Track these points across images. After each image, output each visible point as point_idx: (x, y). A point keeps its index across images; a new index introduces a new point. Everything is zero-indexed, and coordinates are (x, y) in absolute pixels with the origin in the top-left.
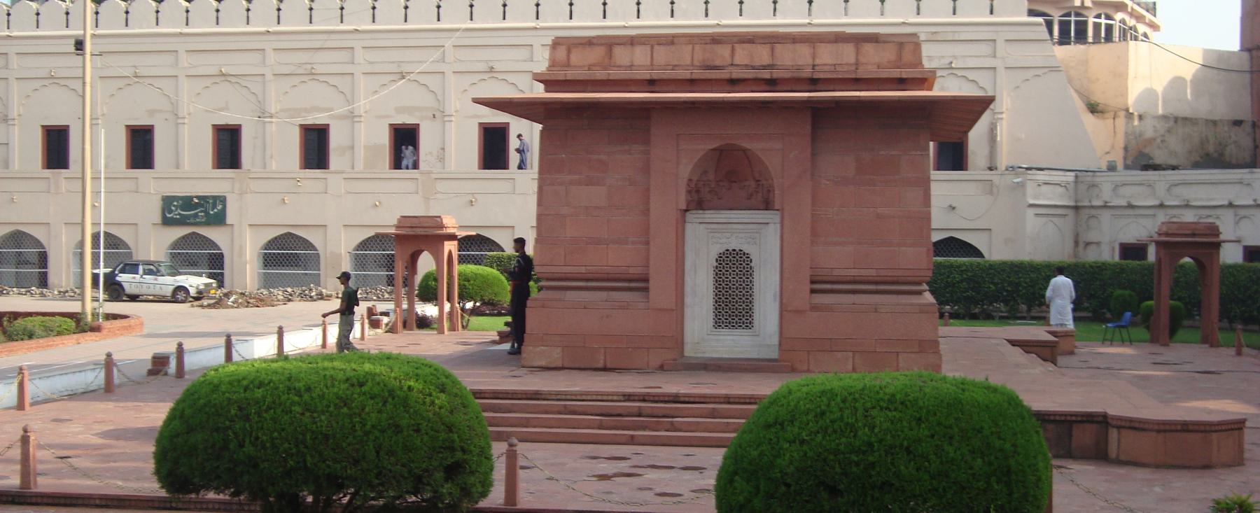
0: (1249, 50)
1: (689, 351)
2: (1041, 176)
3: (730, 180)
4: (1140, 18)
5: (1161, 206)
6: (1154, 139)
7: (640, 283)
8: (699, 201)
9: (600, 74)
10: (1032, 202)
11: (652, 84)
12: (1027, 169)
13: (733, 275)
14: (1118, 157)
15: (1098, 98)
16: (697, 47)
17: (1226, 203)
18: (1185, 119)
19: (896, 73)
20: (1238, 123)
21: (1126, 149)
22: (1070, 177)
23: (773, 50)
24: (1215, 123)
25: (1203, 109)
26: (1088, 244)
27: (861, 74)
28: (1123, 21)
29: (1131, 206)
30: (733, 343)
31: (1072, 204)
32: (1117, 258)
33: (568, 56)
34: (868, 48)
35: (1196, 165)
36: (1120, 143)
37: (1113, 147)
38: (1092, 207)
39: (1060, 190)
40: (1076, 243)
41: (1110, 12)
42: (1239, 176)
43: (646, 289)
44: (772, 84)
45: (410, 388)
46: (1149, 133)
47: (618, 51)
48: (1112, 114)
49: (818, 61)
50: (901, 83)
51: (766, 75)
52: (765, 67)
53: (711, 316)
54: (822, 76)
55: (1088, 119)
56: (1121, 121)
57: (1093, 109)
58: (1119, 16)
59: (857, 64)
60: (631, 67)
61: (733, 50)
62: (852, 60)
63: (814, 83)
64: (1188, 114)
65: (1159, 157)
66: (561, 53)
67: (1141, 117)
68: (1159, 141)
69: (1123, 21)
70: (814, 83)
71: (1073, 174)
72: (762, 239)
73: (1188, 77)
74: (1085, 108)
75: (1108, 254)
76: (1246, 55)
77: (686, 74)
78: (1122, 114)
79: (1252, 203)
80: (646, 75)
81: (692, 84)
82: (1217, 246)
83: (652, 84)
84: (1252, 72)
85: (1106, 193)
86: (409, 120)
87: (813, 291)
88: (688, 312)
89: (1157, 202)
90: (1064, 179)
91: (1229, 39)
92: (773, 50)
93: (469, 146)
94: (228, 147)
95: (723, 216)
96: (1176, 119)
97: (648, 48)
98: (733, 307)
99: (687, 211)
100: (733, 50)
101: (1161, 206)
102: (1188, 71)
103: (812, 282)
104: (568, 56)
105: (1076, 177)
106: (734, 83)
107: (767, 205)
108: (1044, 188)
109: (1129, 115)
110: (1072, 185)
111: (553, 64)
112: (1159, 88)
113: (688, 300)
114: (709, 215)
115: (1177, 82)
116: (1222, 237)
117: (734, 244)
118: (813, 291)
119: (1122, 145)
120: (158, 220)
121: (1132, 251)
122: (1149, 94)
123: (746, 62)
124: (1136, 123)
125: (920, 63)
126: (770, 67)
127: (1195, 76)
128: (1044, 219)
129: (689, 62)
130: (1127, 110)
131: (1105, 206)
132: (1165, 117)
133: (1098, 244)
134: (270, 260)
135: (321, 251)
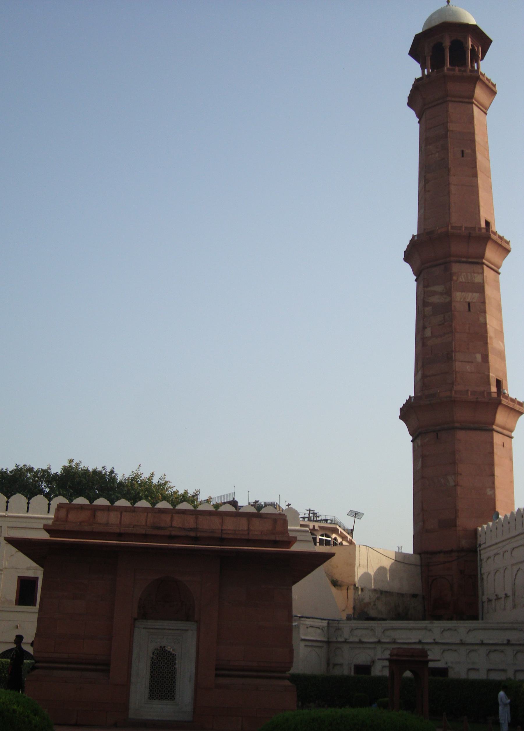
0: (420, 554)
1: (132, 715)
2: (309, 622)
3: (166, 602)
4: (344, 538)
5: (379, 642)
6: (370, 603)
8: (144, 614)
9: (87, 528)
10: (303, 637)
12: (300, 617)
14: (350, 611)
15: (338, 577)
16: (150, 515)
17: (417, 641)
18: (386, 592)
19: (273, 538)
20: (414, 596)
21: (354, 608)
22: (325, 623)
23: (197, 519)
24: (402, 595)
25: (396, 586)
26: (335, 665)
28: (335, 539)
29: (361, 642)
30: (160, 710)
31: (325, 639)
32: (352, 674)
33: (67, 516)
34: (256, 522)
35: (393, 619)
36: (351, 604)
37: (347, 607)
38: (338, 642)
39: (319, 631)
40: (328, 664)
41: (328, 533)
42: (424, 625)
44: (196, 540)
45: (14, 711)
46: (367, 600)
47: (99, 514)
48: (347, 587)
49: (225, 527)
50: (275, 543)
51: (193, 534)
52: (191, 530)
53: (147, 691)
54: (227, 537)
55: (333, 589)
56: (351, 592)
57: (335, 583)
58: (334, 536)
59: (249, 530)
60: (107, 524)
61: (172, 518)
62: (246, 528)
64: (387, 588)
65: (372, 613)
66: (63, 513)
67: (362, 590)
68: (372, 604)
69: (335, 539)
70: (222, 540)
71: (326, 621)
73: (388, 567)
74: (329, 582)
75: (347, 671)
76: (418, 556)
77: (143, 532)
78: (352, 587)
79: (433, 641)
81: (145, 537)
82: (427, 662)
83: (120, 536)
84: (421, 566)
85: (346, 634)
87: (217, 675)
88: (132, 688)
89: (376, 640)
90: (321, 624)
91: (409, 549)
92: (197, 519)
95: (159, 624)
96: (382, 592)
97: (119, 513)
99: (135, 619)
100: (172, 518)
101: (379, 642)
102: (387, 564)
103: (217, 669)
104: (67, 516)
105: (328, 623)
106: (172, 538)
107: (188, 618)
108: (310, 630)
109: (356, 588)
110: (326, 628)
111: (57, 519)
112: (372, 573)
113: (133, 680)
114: (150, 623)
115: (382, 570)
116: (430, 658)
118: (217, 675)
119: (352, 606)
121: (363, 669)
122: (366, 575)
123: (180, 525)
124: (360, 593)
125: (287, 531)
126: (195, 530)
127: (390, 567)
128: (309, 649)
129: (144, 524)
130: (355, 585)
131: (346, 642)
132: (375, 590)
133: (341, 665)
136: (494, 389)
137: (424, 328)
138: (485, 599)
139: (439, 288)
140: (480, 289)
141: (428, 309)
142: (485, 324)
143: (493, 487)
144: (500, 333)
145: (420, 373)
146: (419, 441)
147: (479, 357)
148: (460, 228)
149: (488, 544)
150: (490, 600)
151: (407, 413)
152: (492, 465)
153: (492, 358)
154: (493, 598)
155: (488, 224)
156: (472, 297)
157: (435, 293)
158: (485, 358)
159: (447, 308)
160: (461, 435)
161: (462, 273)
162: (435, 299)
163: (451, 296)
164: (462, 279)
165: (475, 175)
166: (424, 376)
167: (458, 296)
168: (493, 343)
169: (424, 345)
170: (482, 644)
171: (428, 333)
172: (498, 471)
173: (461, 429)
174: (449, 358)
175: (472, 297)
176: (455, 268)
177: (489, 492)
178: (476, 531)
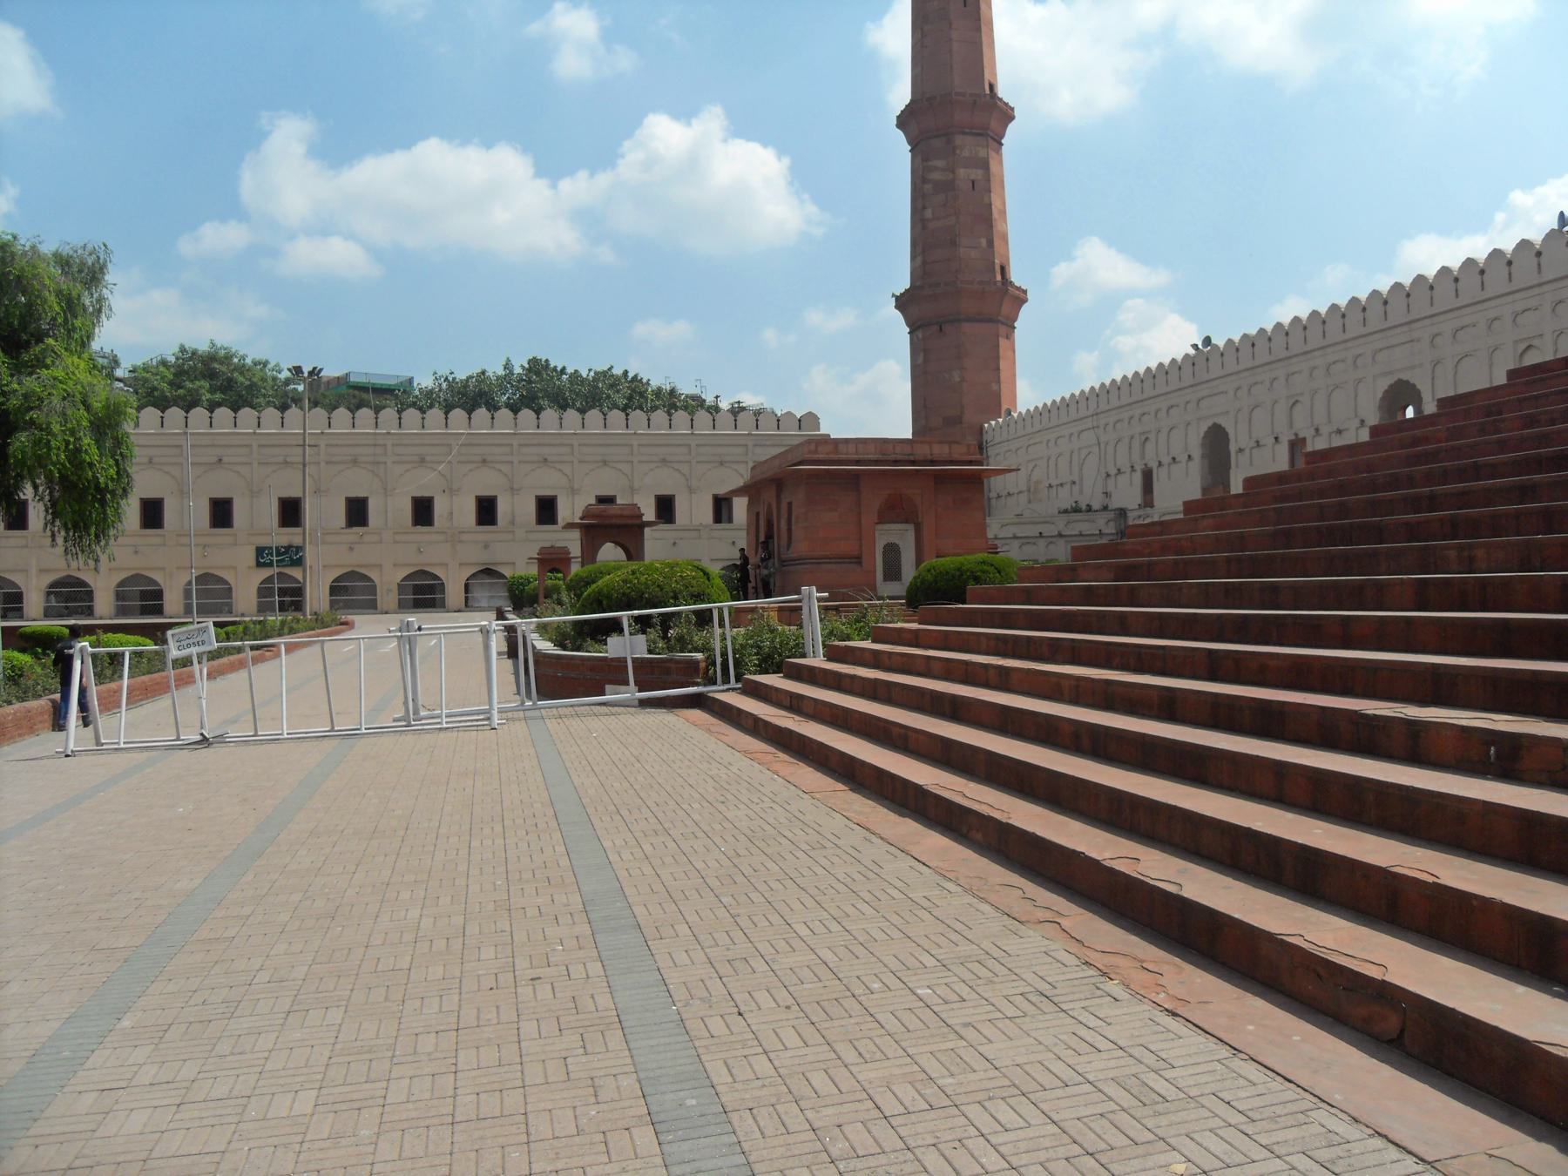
3: (896, 510)
7: (858, 560)
9: (833, 456)
11: (858, 462)
13: (892, 552)
27: (956, 457)
43: (860, 563)
44: (913, 463)
50: (971, 463)
63: (932, 463)
72: (903, 536)
77: (876, 457)
80: (856, 457)
81: (877, 462)
86: (426, 494)
93: (467, 512)
94: (290, 512)
98: (893, 573)
106: (896, 462)
117: (892, 540)
120: (253, 562)
134: (335, 590)
135: (377, 581)
136: (999, 278)
137: (924, 208)
138: (993, 495)
139: (940, 163)
140: (985, 165)
141: (928, 187)
142: (990, 205)
143: (998, 382)
144: (1003, 213)
145: (919, 260)
146: (920, 334)
147: (984, 242)
148: (963, 95)
149: (997, 439)
150: (999, 496)
151: (902, 302)
152: (997, 358)
153: (997, 242)
154: (1004, 493)
155: (992, 87)
156: (977, 174)
157: (936, 169)
158: (991, 243)
159: (948, 186)
160: (967, 327)
161: (967, 146)
162: (935, 176)
163: (953, 171)
164: (966, 153)
165: (979, 29)
166: (924, 263)
167: (962, 172)
168: (998, 226)
169: (924, 228)
170: (1015, 537)
171: (928, 214)
172: (1003, 365)
173: (969, 320)
174: (954, 243)
175: (977, 174)
176: (959, 140)
177: (995, 387)
178: (982, 428)
